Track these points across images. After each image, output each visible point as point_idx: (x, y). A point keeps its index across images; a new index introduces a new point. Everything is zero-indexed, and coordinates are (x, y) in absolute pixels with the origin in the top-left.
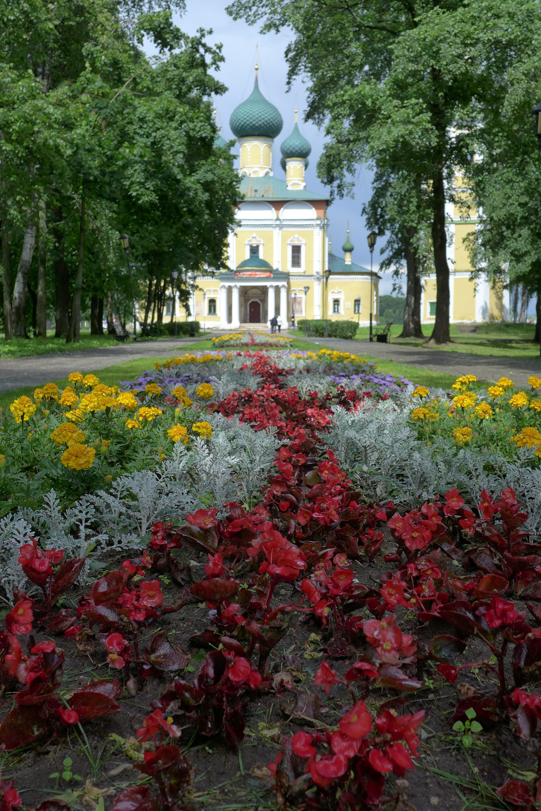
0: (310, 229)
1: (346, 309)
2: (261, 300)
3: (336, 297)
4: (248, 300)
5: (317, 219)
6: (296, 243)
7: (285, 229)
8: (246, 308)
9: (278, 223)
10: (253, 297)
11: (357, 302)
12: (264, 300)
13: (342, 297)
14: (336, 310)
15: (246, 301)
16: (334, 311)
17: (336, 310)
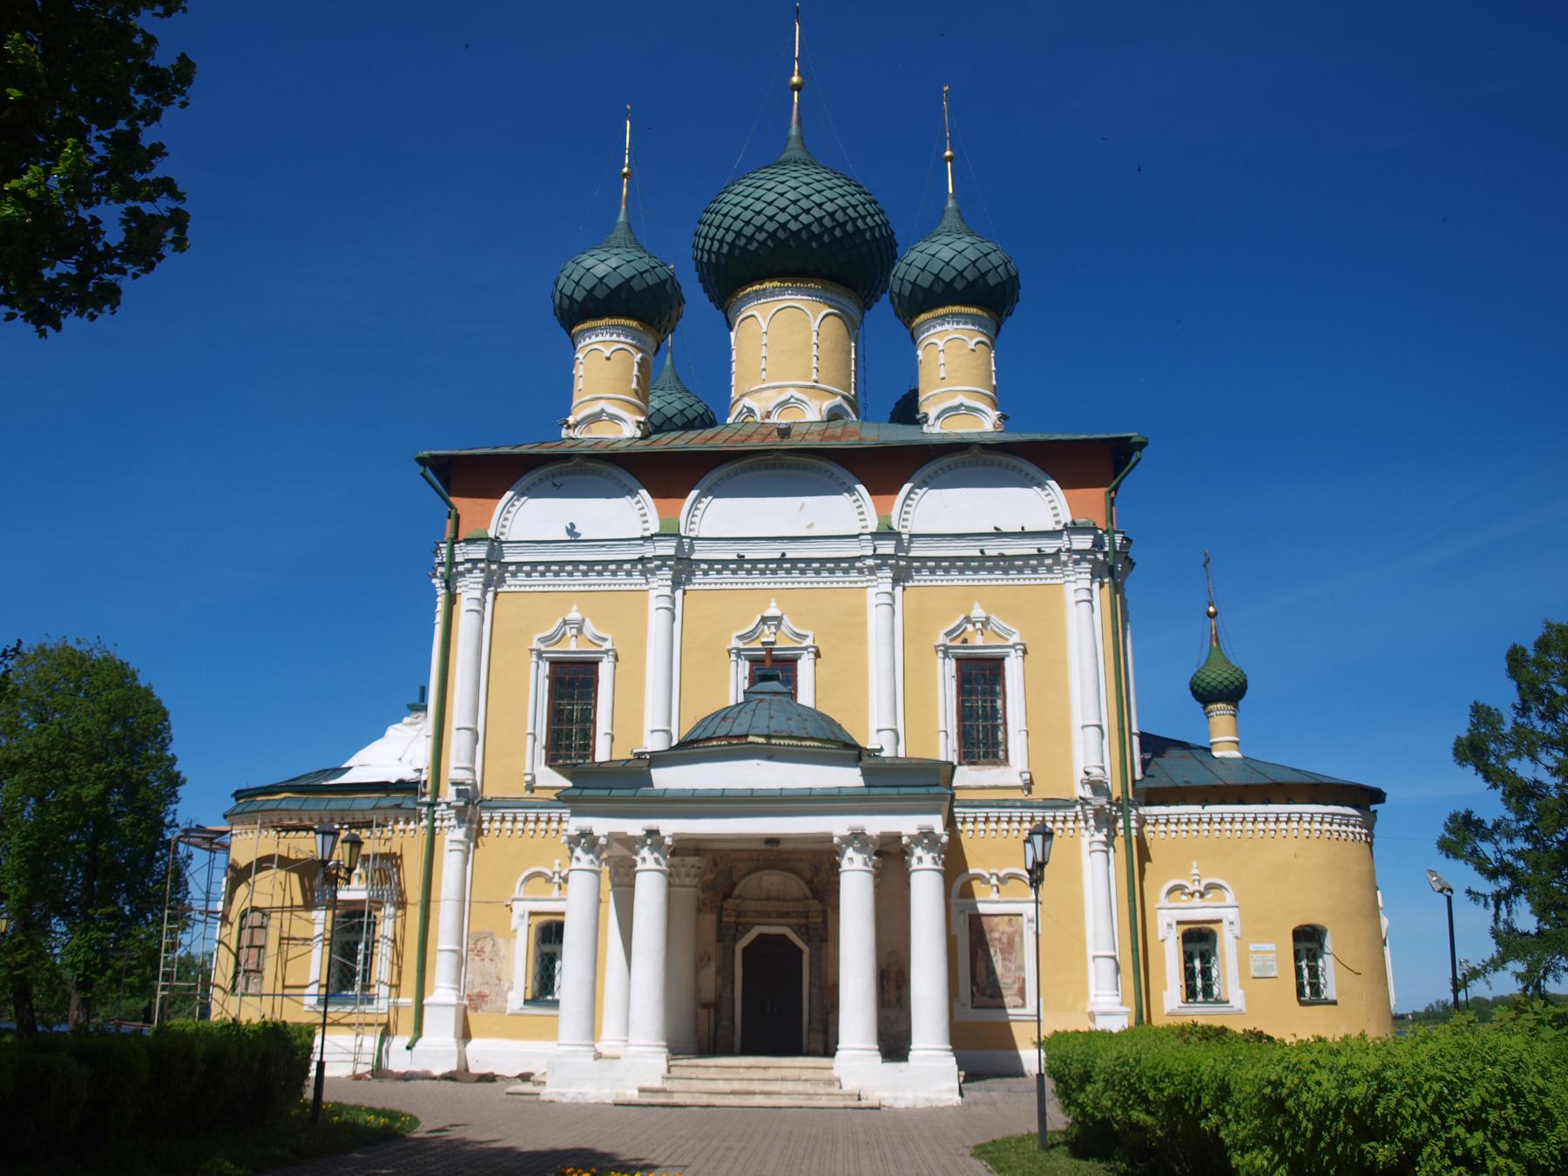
0: (1043, 578)
1: (1252, 980)
2: (803, 930)
3: (1199, 912)
4: (741, 929)
5: (1074, 529)
6: (979, 642)
7: (922, 579)
8: (725, 971)
9: (887, 547)
10: (764, 917)
11: (1308, 940)
12: (823, 931)
13: (1224, 913)
14: (1198, 984)
15: (726, 934)
16: (1191, 993)
17: (1198, 984)
